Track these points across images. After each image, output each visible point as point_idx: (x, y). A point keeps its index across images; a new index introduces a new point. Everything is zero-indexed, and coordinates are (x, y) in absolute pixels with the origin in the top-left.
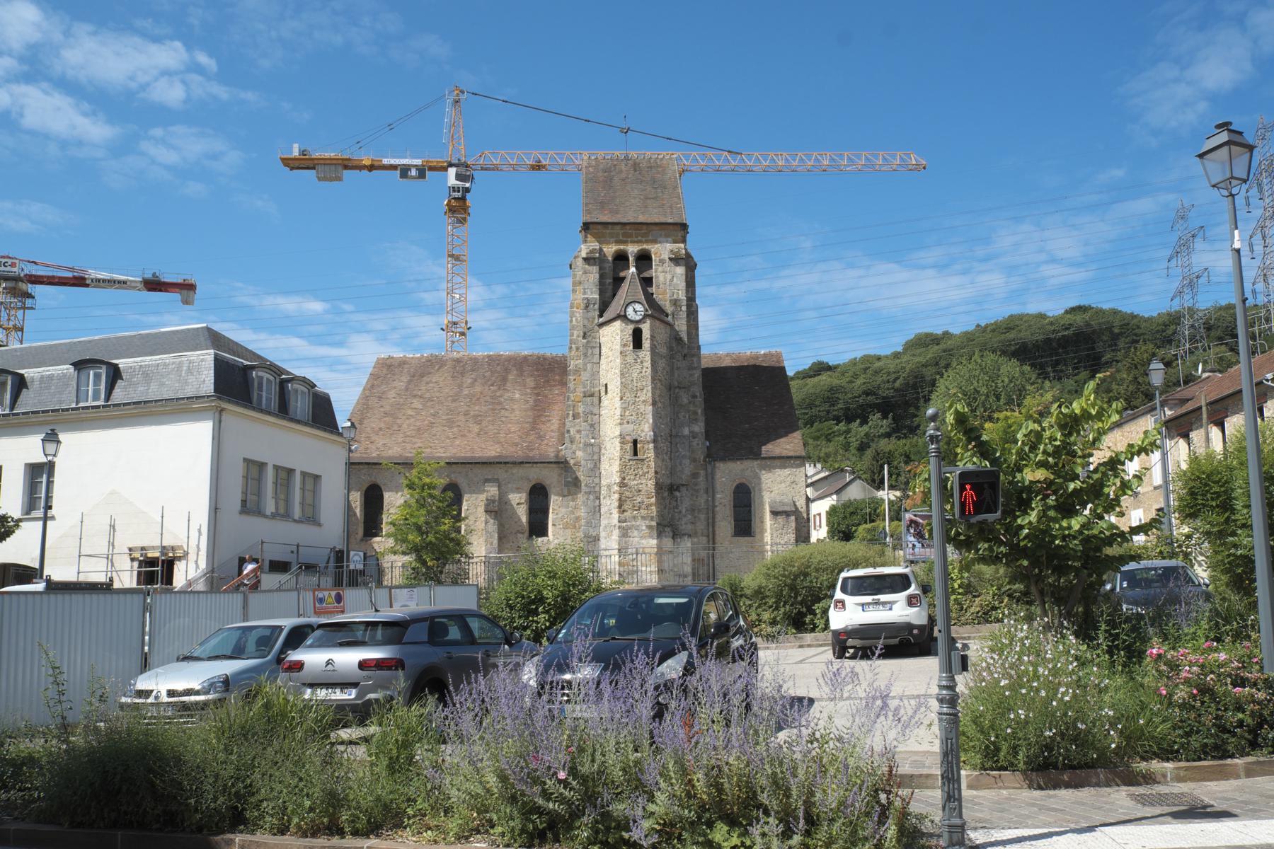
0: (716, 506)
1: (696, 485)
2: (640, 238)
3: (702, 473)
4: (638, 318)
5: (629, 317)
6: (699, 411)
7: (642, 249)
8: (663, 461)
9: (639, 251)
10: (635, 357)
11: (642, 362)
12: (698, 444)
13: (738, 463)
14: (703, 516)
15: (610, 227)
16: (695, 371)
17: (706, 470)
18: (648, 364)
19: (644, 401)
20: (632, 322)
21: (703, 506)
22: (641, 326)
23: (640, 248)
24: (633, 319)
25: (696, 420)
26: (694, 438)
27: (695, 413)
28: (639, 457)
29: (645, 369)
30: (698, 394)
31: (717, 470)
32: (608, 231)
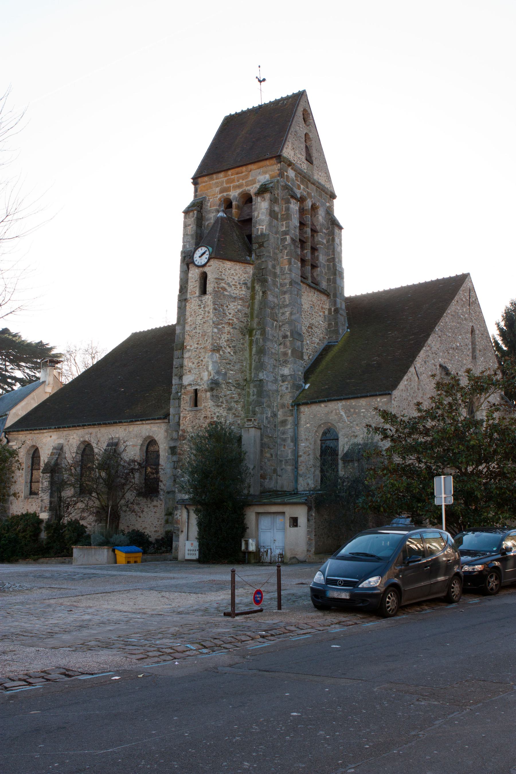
0: (301, 456)
1: (284, 433)
2: (241, 181)
3: (290, 419)
4: (203, 263)
5: (196, 263)
6: (290, 351)
7: (242, 191)
8: (230, 409)
9: (239, 194)
10: (199, 302)
11: (204, 307)
12: (287, 388)
13: (323, 405)
14: (289, 468)
15: (215, 176)
16: (286, 309)
17: (292, 415)
18: (210, 308)
19: (204, 348)
20: (199, 267)
21: (290, 456)
22: (206, 269)
23: (241, 190)
24: (200, 264)
25: (286, 362)
26: (283, 381)
27: (285, 354)
28: (199, 408)
29: (207, 314)
30: (289, 334)
31: (302, 415)
32: (214, 182)
